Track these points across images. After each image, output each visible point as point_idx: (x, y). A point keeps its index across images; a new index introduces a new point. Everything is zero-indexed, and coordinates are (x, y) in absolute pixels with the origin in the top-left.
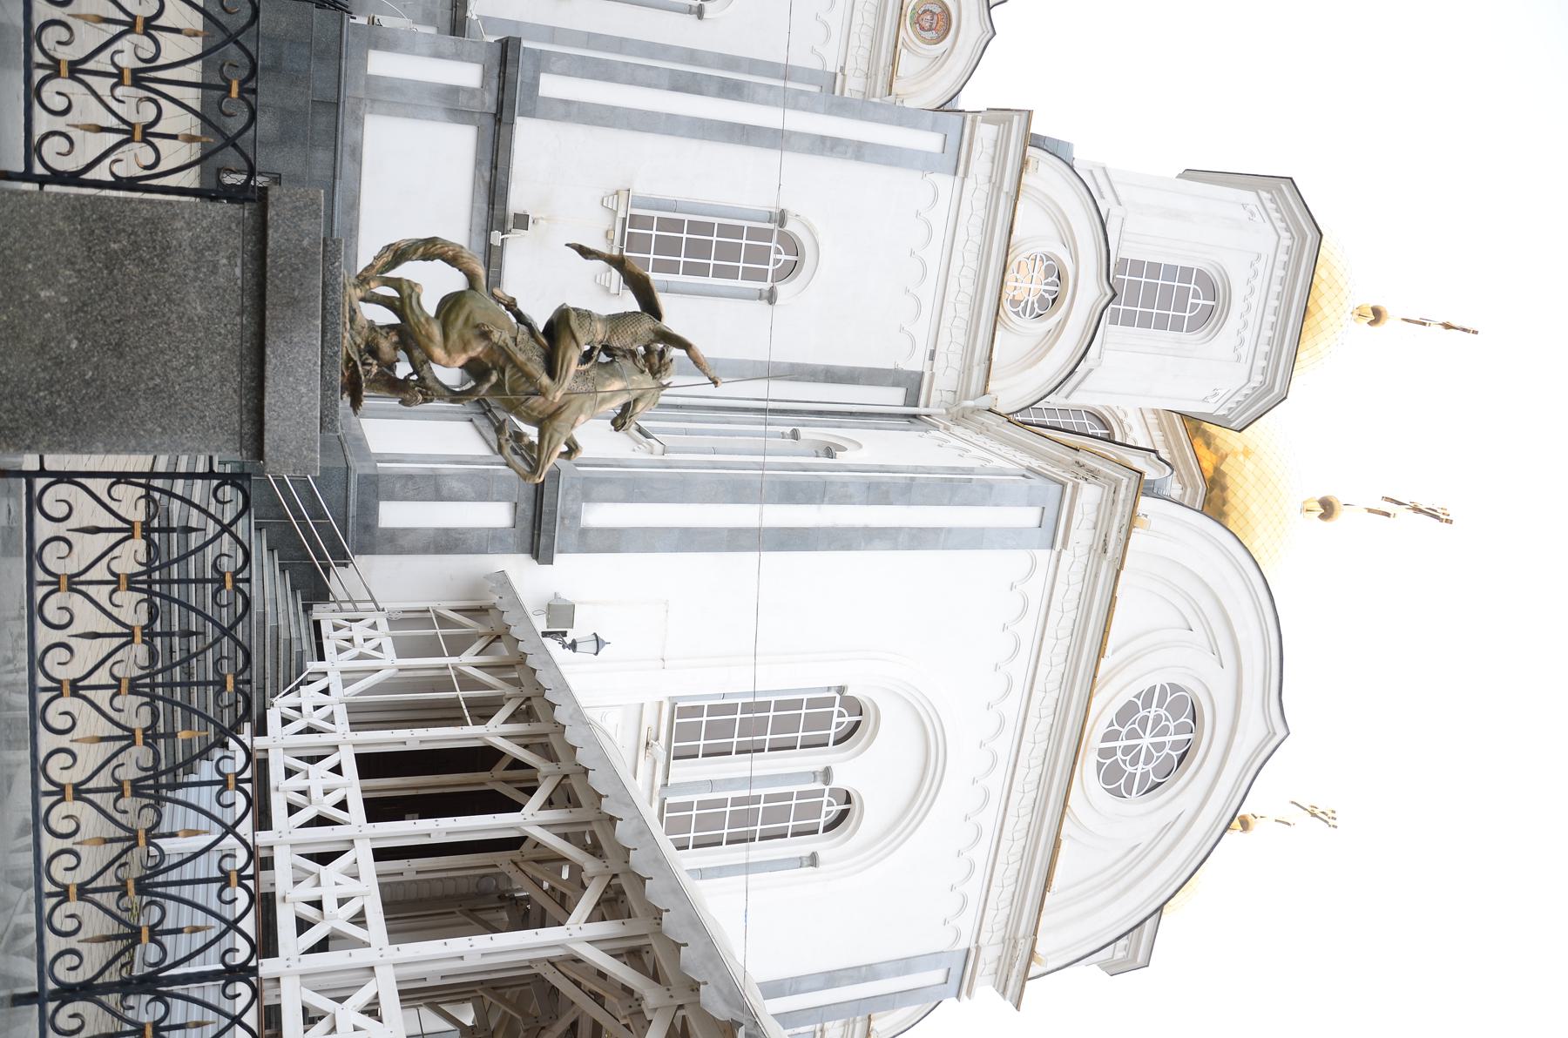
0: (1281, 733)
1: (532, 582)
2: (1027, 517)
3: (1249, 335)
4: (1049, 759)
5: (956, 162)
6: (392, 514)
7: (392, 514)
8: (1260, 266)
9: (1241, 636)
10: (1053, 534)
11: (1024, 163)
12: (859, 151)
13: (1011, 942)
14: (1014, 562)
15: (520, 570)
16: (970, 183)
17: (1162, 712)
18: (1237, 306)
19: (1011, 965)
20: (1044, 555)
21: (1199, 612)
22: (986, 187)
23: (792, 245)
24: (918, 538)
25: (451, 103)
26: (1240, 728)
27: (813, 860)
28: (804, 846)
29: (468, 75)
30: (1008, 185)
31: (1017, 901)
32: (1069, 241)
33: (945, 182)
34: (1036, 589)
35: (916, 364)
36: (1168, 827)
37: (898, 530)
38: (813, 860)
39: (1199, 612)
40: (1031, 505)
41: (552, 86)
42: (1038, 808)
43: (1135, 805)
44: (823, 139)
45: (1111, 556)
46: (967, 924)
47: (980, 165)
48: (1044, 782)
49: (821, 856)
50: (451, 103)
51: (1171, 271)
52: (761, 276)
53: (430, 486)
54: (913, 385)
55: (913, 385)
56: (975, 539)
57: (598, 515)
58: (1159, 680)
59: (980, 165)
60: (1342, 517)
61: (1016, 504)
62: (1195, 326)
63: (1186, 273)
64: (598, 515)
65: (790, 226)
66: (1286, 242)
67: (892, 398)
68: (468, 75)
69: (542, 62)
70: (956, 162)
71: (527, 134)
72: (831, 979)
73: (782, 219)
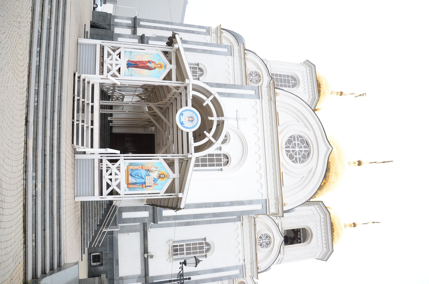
0: (331, 149)
2: (253, 92)
3: (306, 87)
4: (273, 149)
5: (231, 53)
8: (304, 73)
9: (311, 123)
10: (258, 95)
11: (245, 54)
12: (211, 52)
13: (277, 199)
14: (252, 102)
16: (235, 57)
17: (299, 142)
18: (301, 82)
19: (279, 205)
20: (258, 100)
21: (299, 117)
22: (239, 58)
26: (319, 146)
27: (221, 170)
28: (219, 168)
30: (243, 56)
31: (275, 187)
32: (259, 68)
33: (230, 57)
34: (258, 107)
36: (310, 172)
37: (225, 93)
38: (221, 170)
39: (299, 117)
40: (252, 90)
42: (274, 161)
43: (298, 165)
44: (204, 50)
45: (273, 100)
46: (264, 190)
47: (236, 53)
48: (273, 155)
49: (223, 169)
51: (284, 76)
52: (197, 76)
56: (242, 96)
59: (236, 53)
61: (248, 89)
63: (288, 76)
65: (200, 66)
66: (308, 68)
70: (231, 53)
72: (232, 204)
73: (198, 65)
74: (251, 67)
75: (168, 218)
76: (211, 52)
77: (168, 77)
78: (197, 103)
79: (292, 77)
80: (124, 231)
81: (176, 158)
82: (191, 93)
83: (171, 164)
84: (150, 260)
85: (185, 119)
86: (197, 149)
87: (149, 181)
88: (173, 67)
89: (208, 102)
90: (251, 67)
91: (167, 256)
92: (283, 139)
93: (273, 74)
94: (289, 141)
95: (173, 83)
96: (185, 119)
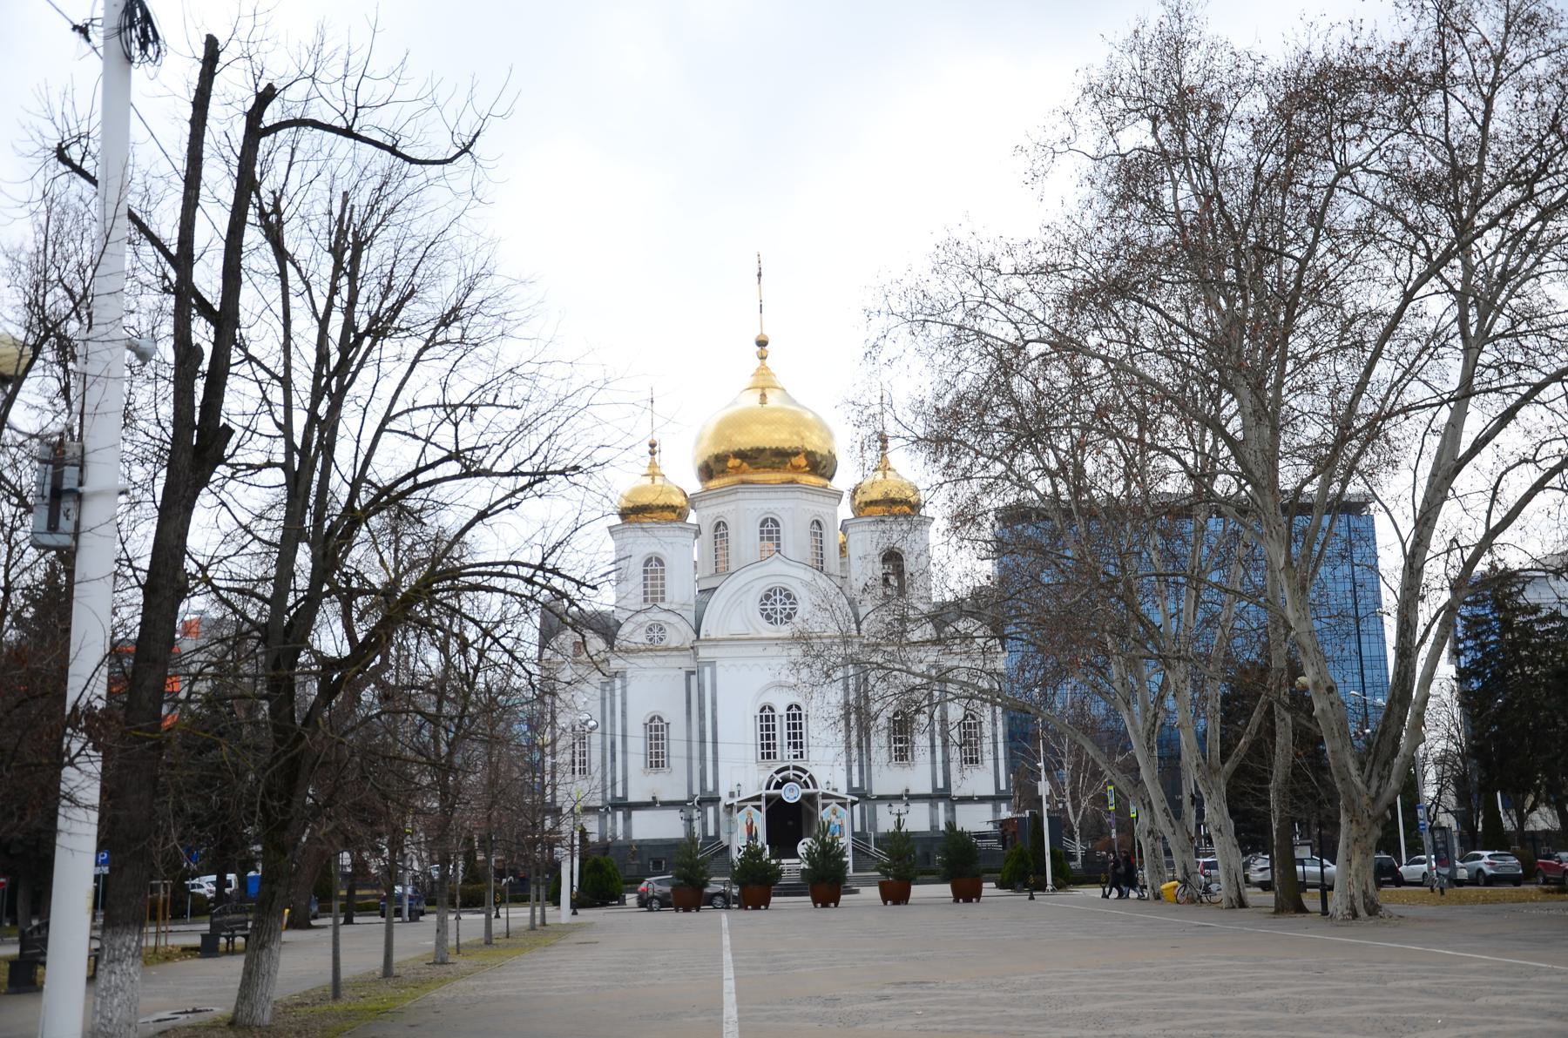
1: (725, 799)
6: (711, 833)
7: (711, 833)
12: (624, 704)
14: (720, 671)
15: (721, 805)
23: (652, 720)
24: (714, 703)
25: (627, 818)
29: (620, 815)
35: (683, 674)
41: (619, 794)
45: (716, 642)
50: (627, 818)
53: (705, 825)
54: (689, 674)
55: (689, 674)
56: (714, 686)
57: (710, 787)
58: (757, 607)
60: (769, 334)
62: (662, 564)
63: (645, 571)
64: (710, 787)
67: (694, 678)
68: (620, 815)
69: (614, 796)
71: (632, 798)
74: (640, 638)
75: (861, 780)
76: (624, 704)
77: (758, 808)
78: (779, 786)
79: (646, 565)
80: (874, 826)
81: (820, 801)
82: (772, 791)
83: (825, 806)
84: (912, 792)
85: (791, 795)
86: (815, 786)
87: (838, 822)
88: (750, 804)
89: (778, 778)
90: (640, 638)
91: (907, 769)
92: (767, 630)
93: (646, 600)
94: (768, 617)
95: (763, 803)
96: (791, 795)
